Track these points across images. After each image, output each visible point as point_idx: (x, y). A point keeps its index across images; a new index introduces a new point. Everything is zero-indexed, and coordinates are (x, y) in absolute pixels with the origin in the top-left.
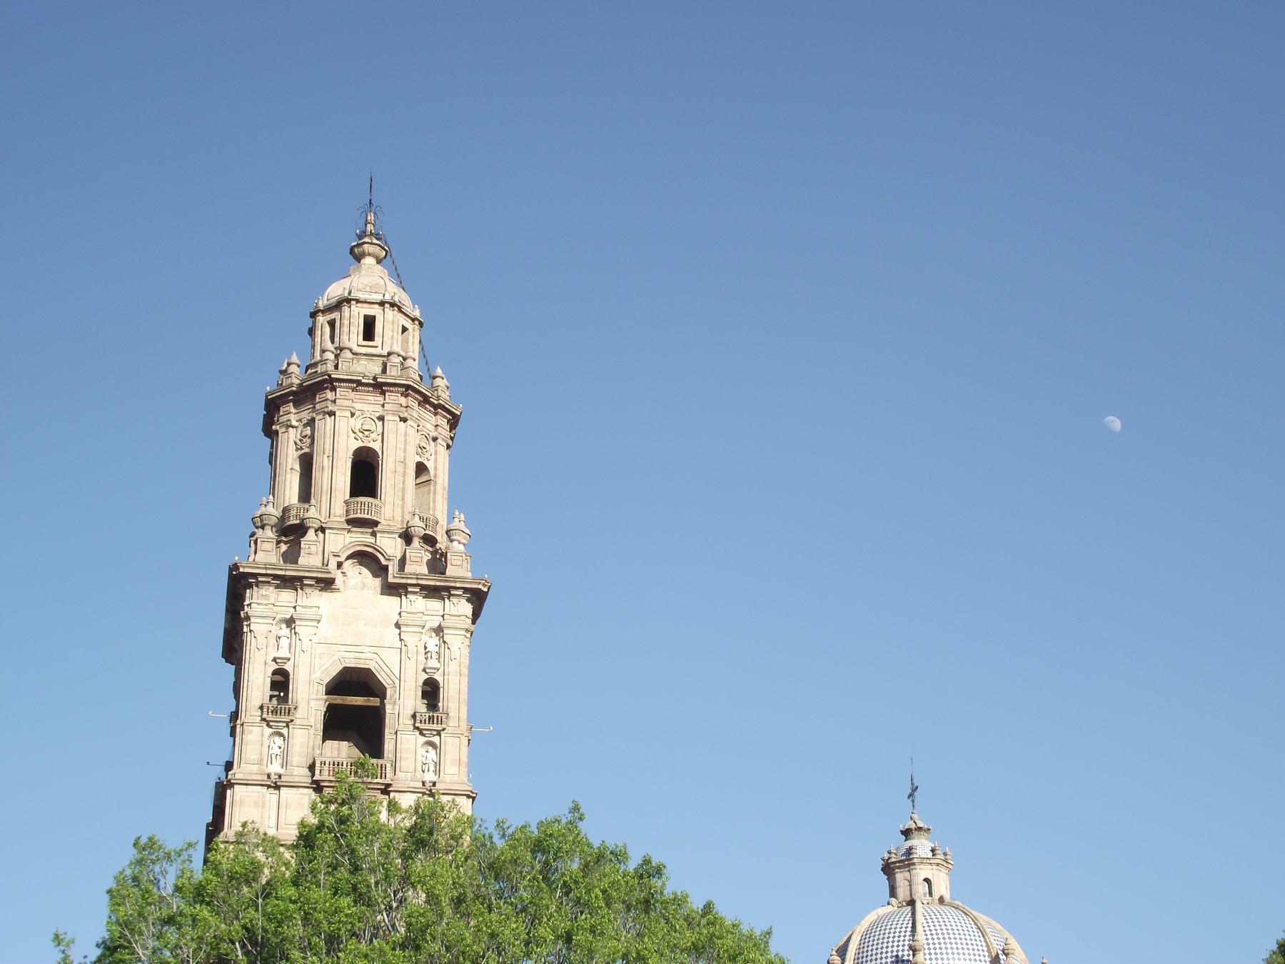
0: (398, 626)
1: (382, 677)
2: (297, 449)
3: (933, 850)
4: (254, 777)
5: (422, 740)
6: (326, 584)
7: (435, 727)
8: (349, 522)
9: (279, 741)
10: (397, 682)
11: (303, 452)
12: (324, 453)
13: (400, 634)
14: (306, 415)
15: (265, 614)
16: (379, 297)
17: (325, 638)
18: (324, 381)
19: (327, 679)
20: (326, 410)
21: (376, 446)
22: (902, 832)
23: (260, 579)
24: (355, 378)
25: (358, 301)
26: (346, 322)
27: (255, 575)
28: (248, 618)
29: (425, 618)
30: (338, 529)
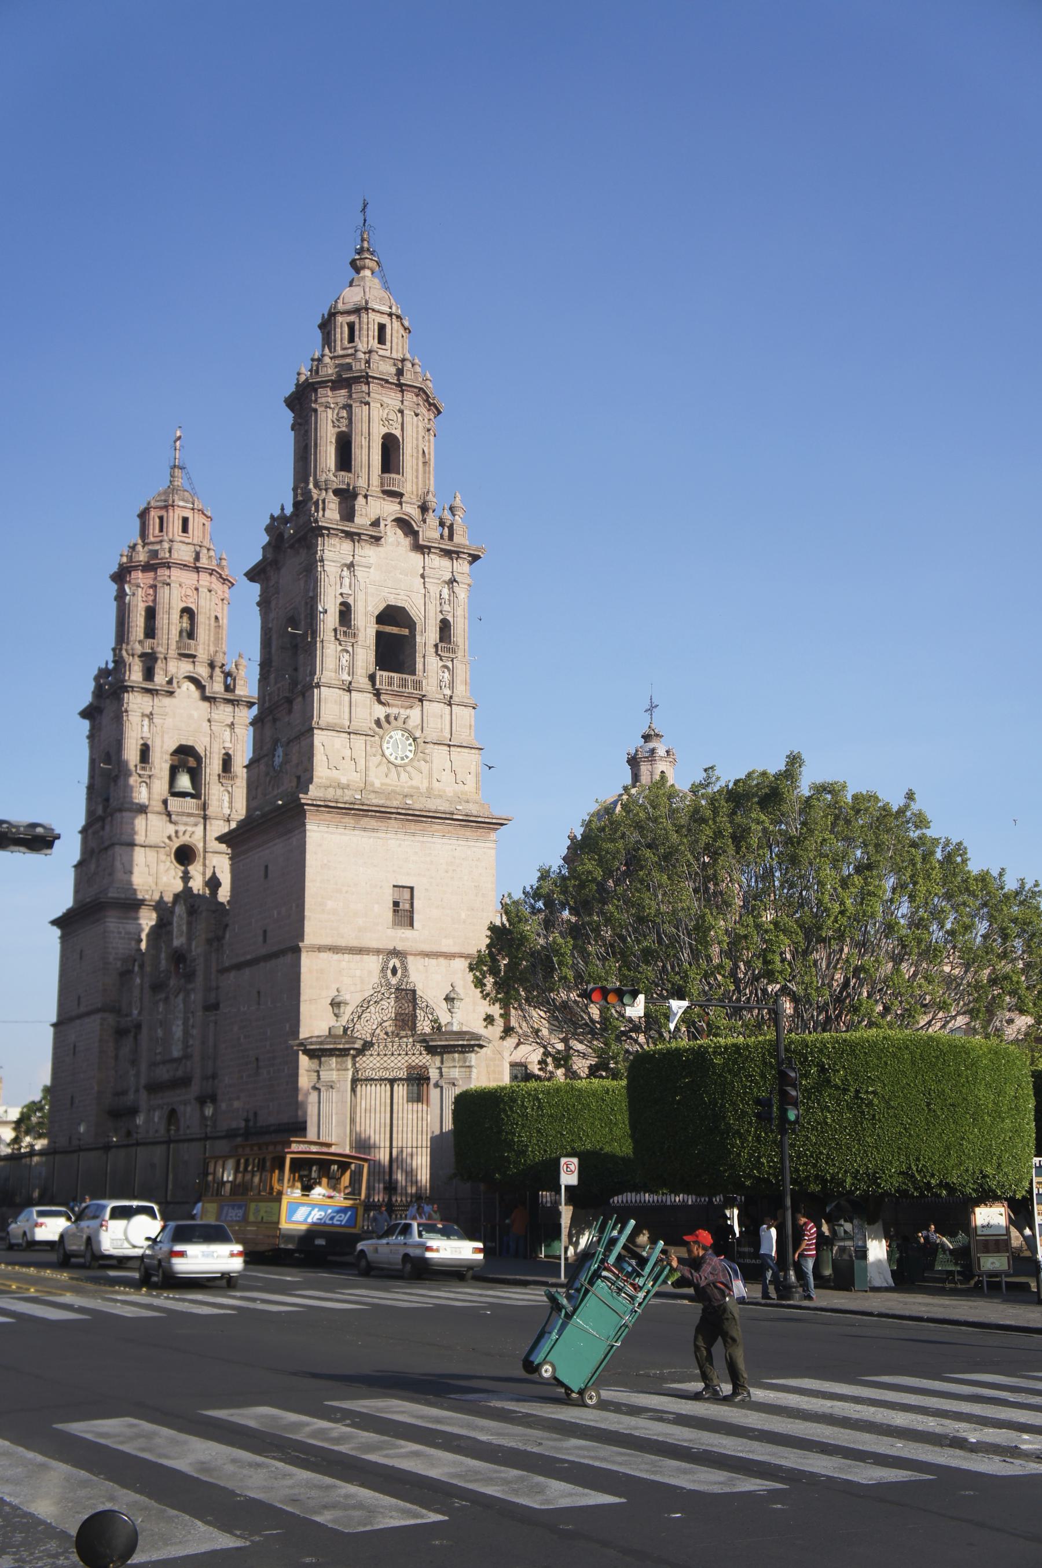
0: (423, 576)
1: (413, 613)
2: (334, 427)
3: (667, 752)
4: (333, 682)
5: (441, 664)
6: (377, 539)
7: (451, 655)
8: (384, 492)
9: (346, 656)
10: (423, 619)
11: (340, 430)
12: (362, 435)
13: (424, 583)
14: (342, 401)
15: (335, 559)
16: (387, 310)
17: (374, 582)
18: (362, 377)
19: (377, 613)
20: (363, 400)
21: (397, 433)
22: (643, 737)
23: (332, 532)
24: (385, 378)
25: (373, 310)
26: (365, 327)
27: (328, 529)
28: (322, 561)
29: (441, 573)
30: (377, 497)
